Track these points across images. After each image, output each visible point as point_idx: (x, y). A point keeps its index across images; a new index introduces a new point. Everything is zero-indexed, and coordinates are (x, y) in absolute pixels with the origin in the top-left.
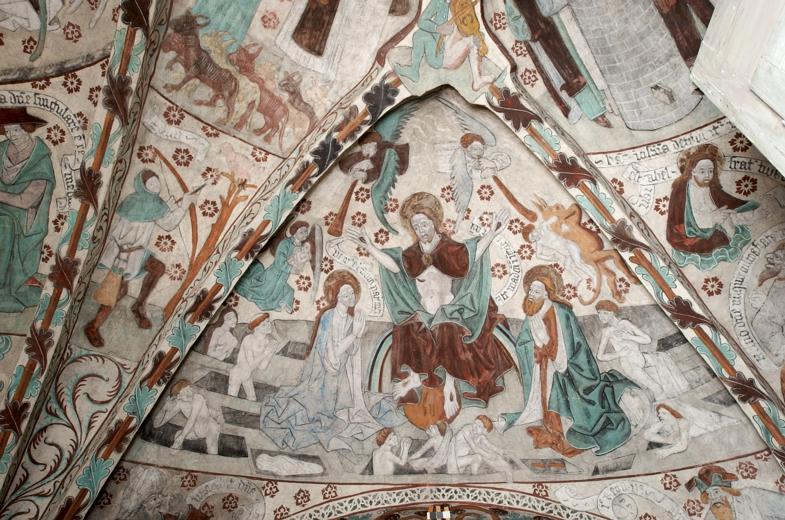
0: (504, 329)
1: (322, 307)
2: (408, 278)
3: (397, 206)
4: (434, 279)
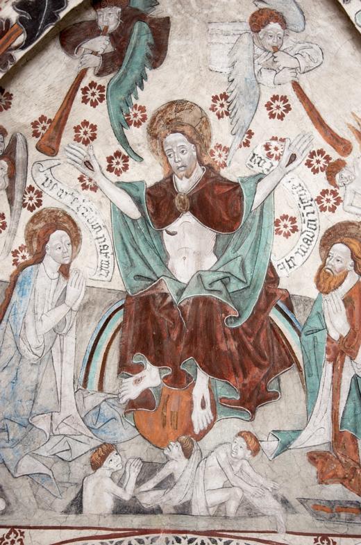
0: (289, 314)
1: (21, 260)
2: (153, 228)
3: (144, 118)
4: (190, 233)
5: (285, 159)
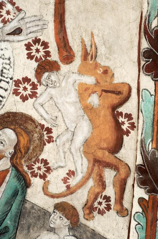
5: (10, 27)
